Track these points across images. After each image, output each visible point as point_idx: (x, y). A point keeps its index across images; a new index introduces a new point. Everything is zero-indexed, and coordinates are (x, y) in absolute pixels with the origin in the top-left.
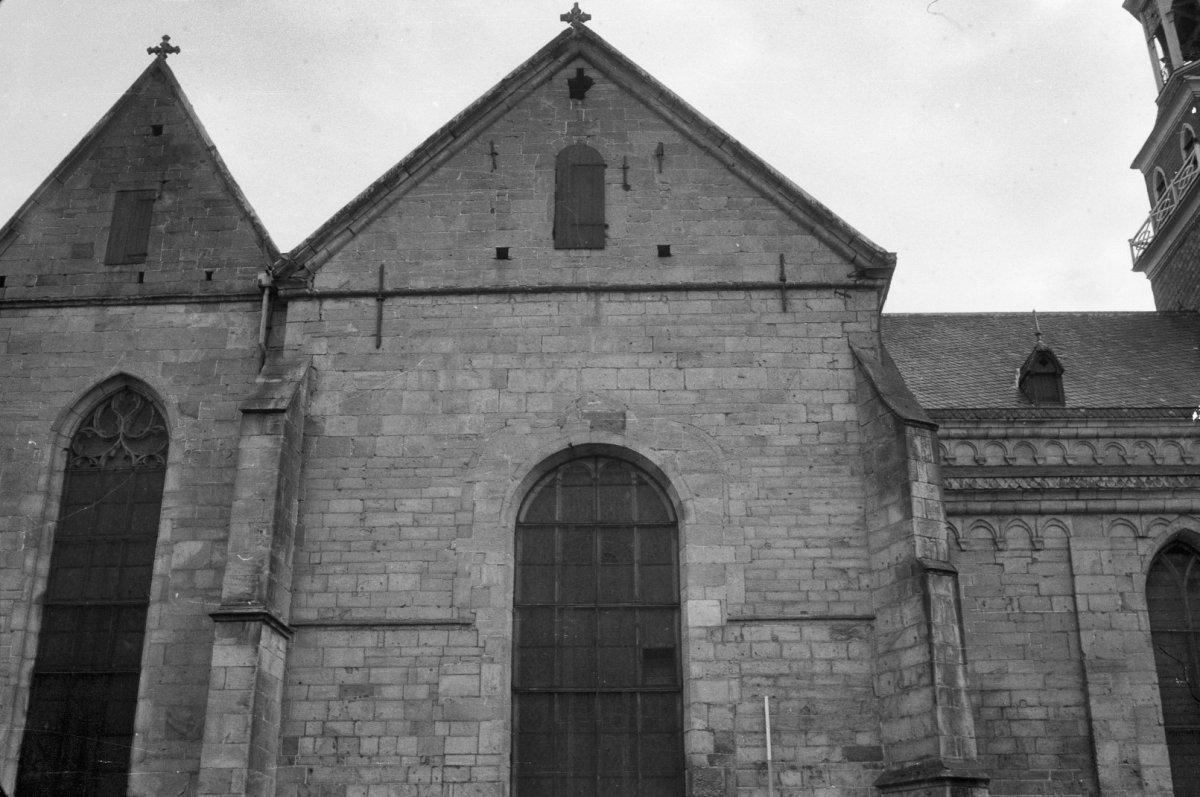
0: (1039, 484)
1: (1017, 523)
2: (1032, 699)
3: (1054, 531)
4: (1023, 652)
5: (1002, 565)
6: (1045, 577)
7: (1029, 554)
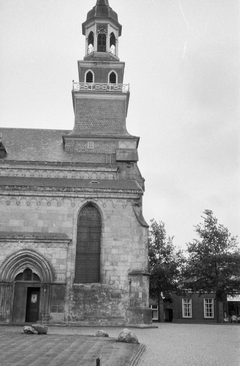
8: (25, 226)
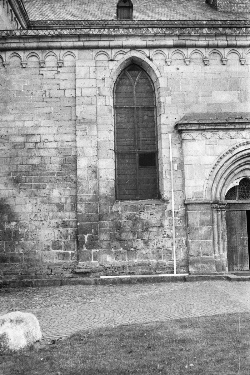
0: (59, 32)
1: (51, 53)
2: (51, 138)
3: (69, 58)
4: (49, 116)
5: (42, 74)
6: (63, 80)
7: (56, 69)
8: (241, 102)
